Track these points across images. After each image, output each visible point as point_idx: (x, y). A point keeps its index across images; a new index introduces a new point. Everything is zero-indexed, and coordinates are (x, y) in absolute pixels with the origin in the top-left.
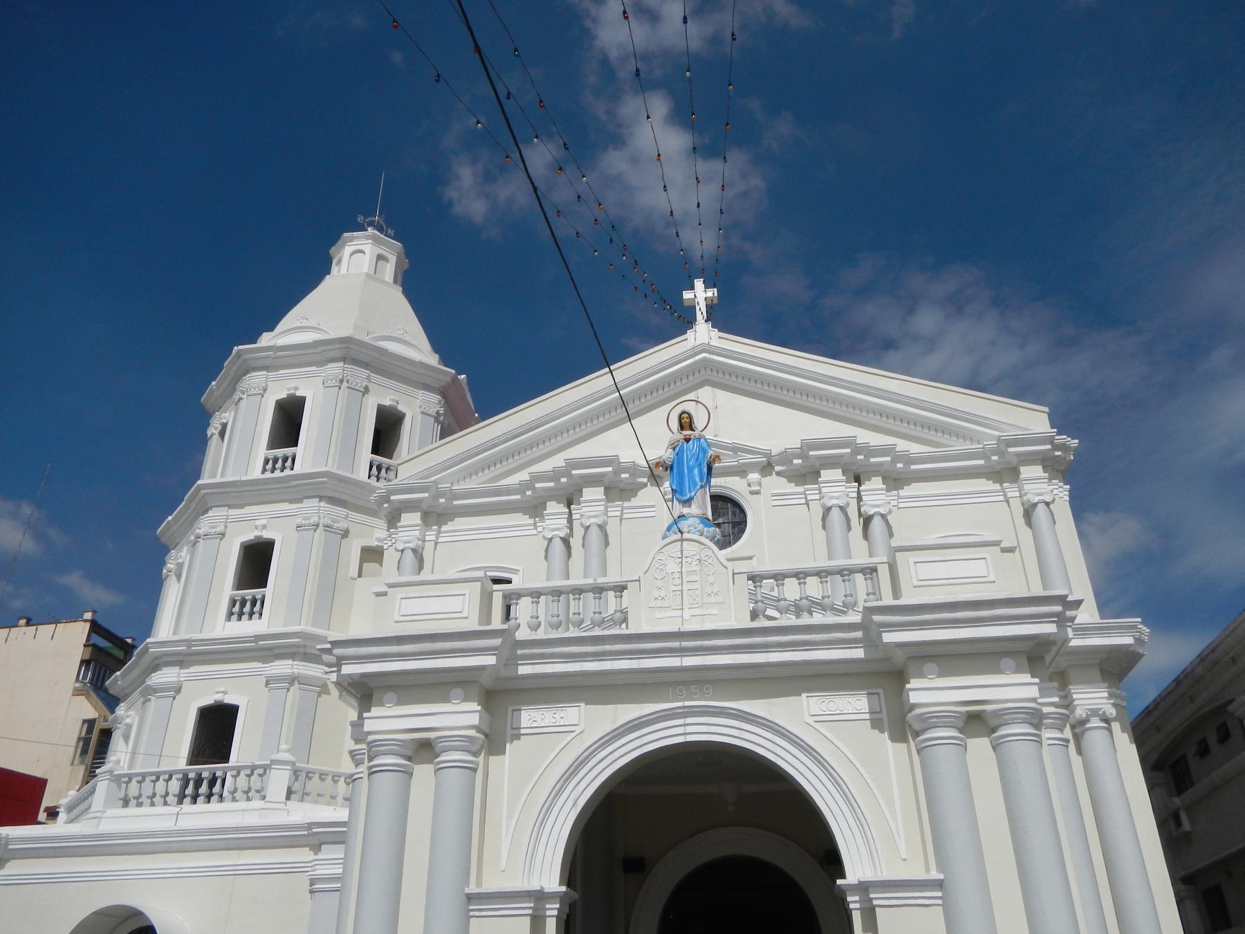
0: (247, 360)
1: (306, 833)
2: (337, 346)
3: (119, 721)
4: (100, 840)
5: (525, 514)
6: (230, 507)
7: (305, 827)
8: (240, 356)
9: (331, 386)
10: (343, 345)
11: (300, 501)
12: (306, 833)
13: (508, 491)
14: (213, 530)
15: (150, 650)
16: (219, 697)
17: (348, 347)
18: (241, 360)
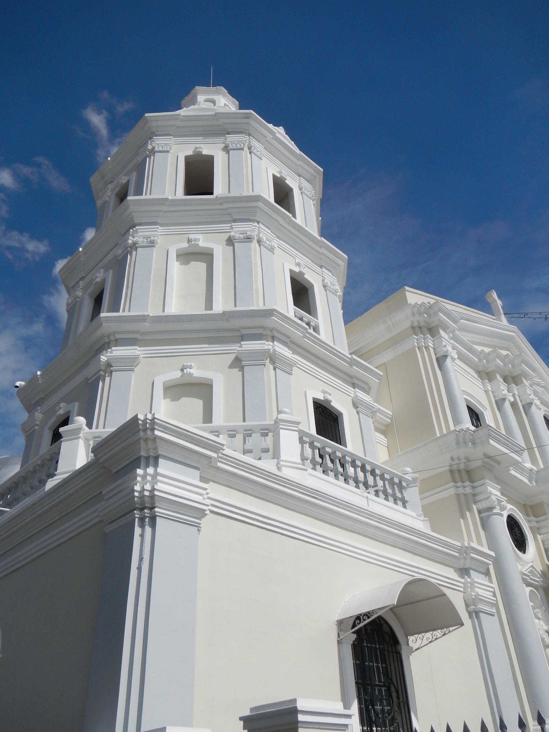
0: (250, 124)
1: (457, 554)
2: (311, 171)
3: (137, 363)
4: (320, 500)
5: (476, 373)
6: (272, 232)
7: (458, 549)
8: (247, 118)
9: (308, 196)
10: (315, 174)
11: (321, 267)
12: (457, 554)
13: (473, 351)
14: (268, 242)
15: (273, 317)
16: (329, 397)
17: (315, 177)
18: (245, 121)
